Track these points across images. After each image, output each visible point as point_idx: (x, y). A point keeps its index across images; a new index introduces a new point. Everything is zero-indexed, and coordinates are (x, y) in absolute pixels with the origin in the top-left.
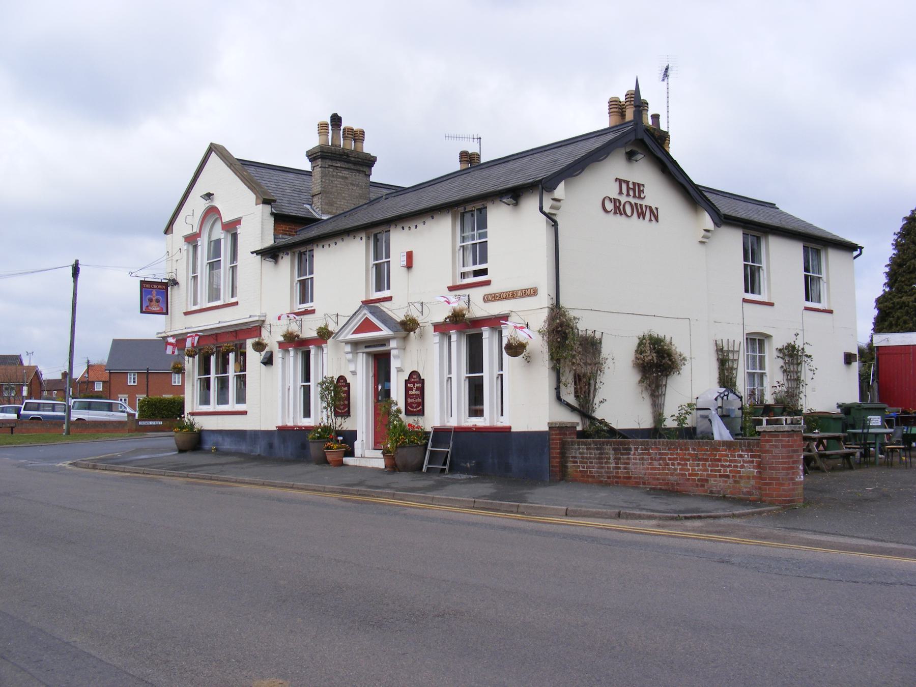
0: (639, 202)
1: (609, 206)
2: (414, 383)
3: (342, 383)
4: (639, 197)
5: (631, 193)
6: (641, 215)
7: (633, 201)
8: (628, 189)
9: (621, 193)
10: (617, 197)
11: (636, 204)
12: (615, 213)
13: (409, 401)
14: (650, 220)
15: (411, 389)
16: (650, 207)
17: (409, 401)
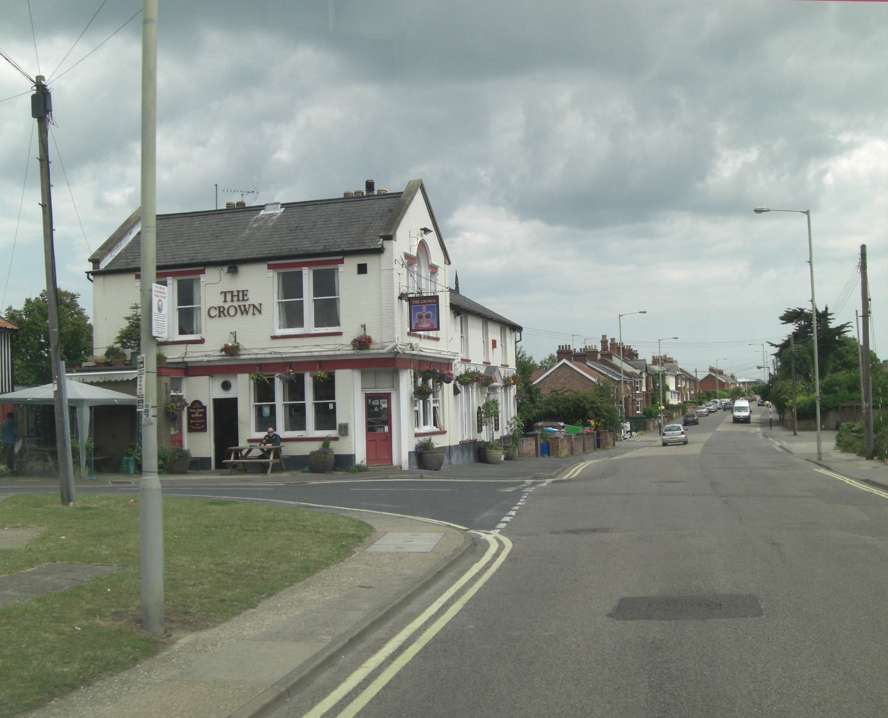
0: (242, 303)
1: (214, 313)
2: (196, 409)
3: (197, 405)
4: (243, 300)
5: (235, 299)
6: (245, 311)
7: (236, 304)
8: (232, 296)
9: (225, 301)
10: (222, 304)
11: (240, 306)
12: (220, 316)
13: (192, 421)
14: (254, 314)
15: (194, 413)
16: (254, 306)
17: (192, 421)
